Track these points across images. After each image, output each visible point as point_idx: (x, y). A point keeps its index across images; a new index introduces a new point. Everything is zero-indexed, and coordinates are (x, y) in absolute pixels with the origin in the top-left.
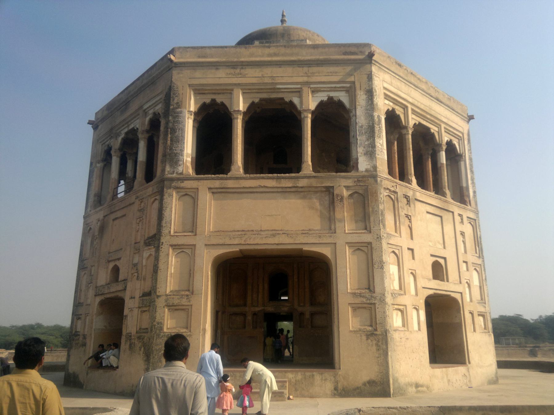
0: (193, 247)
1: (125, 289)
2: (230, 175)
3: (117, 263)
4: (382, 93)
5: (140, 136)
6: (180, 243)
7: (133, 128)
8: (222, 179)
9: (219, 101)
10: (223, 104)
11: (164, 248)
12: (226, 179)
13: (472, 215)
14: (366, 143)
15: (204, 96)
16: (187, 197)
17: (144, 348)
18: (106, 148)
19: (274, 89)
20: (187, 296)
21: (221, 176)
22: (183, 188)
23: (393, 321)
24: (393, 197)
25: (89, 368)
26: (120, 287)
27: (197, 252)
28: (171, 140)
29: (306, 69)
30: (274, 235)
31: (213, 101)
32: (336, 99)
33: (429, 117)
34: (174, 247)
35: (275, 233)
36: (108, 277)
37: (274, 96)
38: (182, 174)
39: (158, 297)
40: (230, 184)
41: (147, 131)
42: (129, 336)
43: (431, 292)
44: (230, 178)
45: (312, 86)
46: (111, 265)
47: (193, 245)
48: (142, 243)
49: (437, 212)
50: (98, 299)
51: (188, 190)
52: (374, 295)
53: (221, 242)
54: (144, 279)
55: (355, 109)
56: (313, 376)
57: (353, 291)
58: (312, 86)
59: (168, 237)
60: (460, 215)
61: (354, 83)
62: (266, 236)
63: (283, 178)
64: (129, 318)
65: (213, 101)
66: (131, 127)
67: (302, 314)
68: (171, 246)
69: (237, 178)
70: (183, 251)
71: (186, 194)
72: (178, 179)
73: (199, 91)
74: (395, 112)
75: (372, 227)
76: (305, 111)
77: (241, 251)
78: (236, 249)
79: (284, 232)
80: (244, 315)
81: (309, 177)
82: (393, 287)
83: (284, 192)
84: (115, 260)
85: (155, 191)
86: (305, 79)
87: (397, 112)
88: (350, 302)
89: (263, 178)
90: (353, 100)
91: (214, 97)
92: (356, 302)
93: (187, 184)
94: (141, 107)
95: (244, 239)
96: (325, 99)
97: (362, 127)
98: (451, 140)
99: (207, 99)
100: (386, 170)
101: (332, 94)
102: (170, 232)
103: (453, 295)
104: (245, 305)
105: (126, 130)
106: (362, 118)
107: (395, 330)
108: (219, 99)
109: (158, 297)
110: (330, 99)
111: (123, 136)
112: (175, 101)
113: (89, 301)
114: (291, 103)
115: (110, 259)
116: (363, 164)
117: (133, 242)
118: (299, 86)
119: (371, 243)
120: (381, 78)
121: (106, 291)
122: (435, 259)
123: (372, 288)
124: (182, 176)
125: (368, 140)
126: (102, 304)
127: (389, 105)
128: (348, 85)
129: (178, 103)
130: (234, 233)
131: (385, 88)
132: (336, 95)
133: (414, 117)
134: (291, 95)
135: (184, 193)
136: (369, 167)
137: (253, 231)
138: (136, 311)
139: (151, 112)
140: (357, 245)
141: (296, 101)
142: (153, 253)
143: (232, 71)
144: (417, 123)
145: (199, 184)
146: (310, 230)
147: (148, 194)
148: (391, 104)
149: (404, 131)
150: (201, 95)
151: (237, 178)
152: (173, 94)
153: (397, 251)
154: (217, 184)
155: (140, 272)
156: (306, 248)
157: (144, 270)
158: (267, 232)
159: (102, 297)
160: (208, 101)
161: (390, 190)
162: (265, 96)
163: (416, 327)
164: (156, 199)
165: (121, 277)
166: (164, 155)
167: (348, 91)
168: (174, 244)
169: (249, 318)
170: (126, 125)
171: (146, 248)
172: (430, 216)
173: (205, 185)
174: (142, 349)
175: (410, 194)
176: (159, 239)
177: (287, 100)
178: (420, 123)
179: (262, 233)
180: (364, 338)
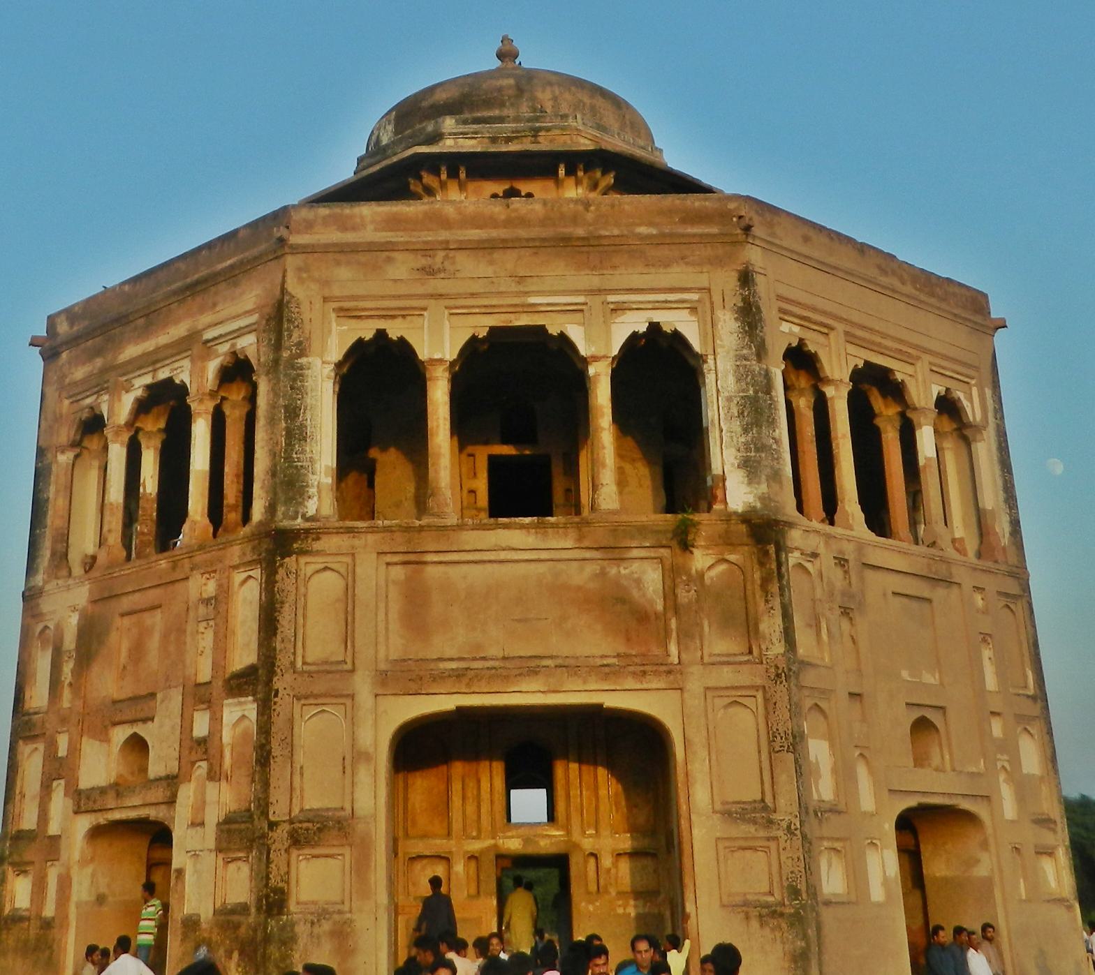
0: (348, 702)
3: (140, 729)
5: (193, 406)
7: (170, 381)
9: (393, 335)
10: (402, 341)
14: (743, 439)
16: (328, 574)
18: (85, 415)
23: (820, 880)
31: (381, 334)
34: (303, 702)
37: (523, 320)
38: (312, 519)
41: (213, 394)
47: (347, 696)
51: (329, 559)
52: (773, 816)
57: (727, 807)
59: (289, 677)
62: (518, 672)
65: (381, 334)
66: (163, 375)
70: (324, 711)
71: (326, 569)
73: (345, 313)
74: (805, 345)
75: (763, 647)
79: (559, 661)
82: (819, 795)
84: (133, 722)
87: (812, 348)
88: (718, 835)
89: (506, 526)
91: (381, 324)
99: (367, 331)
100: (792, 502)
102: (293, 664)
105: (148, 380)
108: (395, 330)
111: (139, 393)
116: (739, 495)
119: (764, 687)
124: (315, 525)
127: (791, 333)
132: (673, 320)
133: (851, 349)
135: (322, 566)
136: (750, 499)
140: (734, 693)
143: (423, 262)
144: (861, 365)
145: (357, 542)
149: (829, 391)
150: (353, 321)
160: (368, 335)
164: (250, 577)
170: (150, 369)
171: (230, 701)
178: (867, 363)
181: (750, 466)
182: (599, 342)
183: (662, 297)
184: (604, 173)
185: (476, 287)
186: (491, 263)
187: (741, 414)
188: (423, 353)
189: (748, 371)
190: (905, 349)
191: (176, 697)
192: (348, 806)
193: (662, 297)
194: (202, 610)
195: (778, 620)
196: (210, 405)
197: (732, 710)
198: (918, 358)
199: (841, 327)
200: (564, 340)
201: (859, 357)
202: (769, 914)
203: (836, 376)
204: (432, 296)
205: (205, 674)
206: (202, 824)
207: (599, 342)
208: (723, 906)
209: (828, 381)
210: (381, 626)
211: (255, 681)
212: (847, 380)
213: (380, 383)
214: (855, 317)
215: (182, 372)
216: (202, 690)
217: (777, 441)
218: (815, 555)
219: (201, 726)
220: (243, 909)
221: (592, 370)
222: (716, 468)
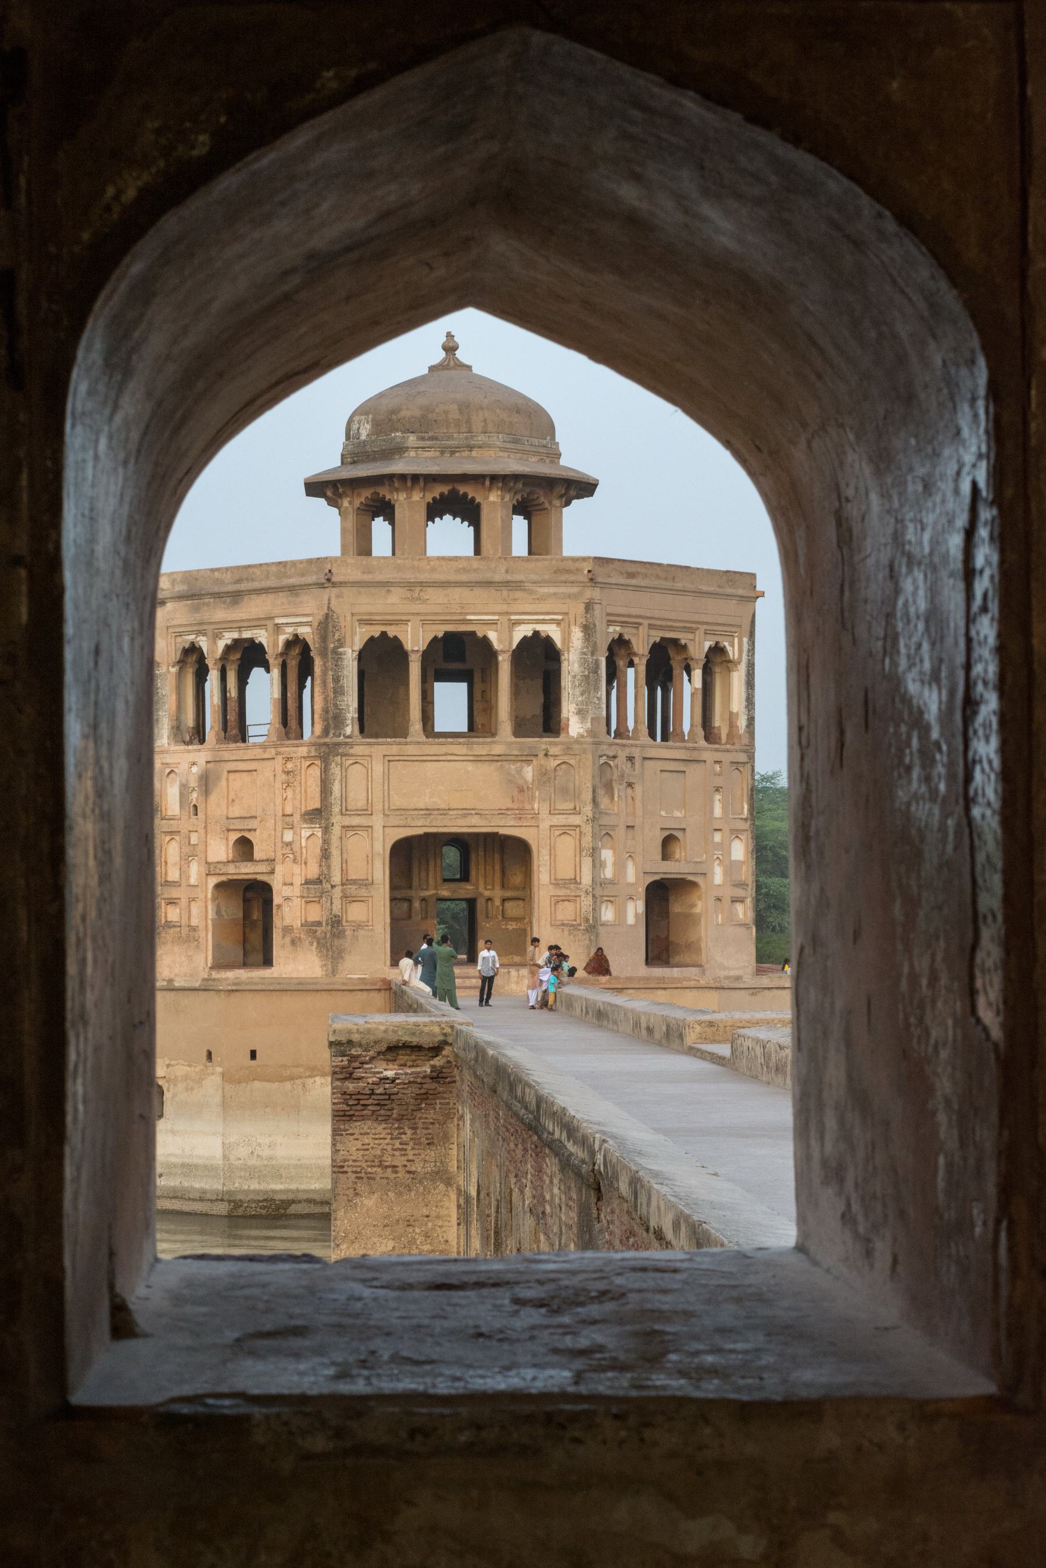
1: (272, 872)
2: (409, 739)
4: (605, 622)
6: (354, 824)
8: (399, 744)
9: (391, 635)
10: (395, 637)
11: (336, 831)
12: (406, 744)
13: (742, 757)
15: (372, 628)
16: (357, 765)
17: (318, 943)
19: (464, 620)
20: (366, 885)
21: (398, 740)
22: (352, 755)
24: (611, 763)
25: (211, 968)
26: (262, 868)
27: (375, 835)
28: (335, 692)
29: (505, 593)
30: (465, 816)
31: (384, 634)
32: (543, 635)
33: (678, 625)
35: (466, 813)
36: (230, 851)
38: (349, 737)
39: (333, 887)
40: (411, 749)
41: (282, 654)
42: (287, 930)
43: (657, 877)
44: (411, 743)
45: (513, 617)
46: (234, 837)
48: (297, 817)
49: (681, 767)
50: (213, 881)
53: (402, 823)
54: (306, 863)
55: (568, 651)
56: (509, 972)
58: (513, 617)
59: (339, 817)
60: (716, 762)
61: (567, 614)
63: (478, 744)
64: (286, 909)
65: (384, 634)
66: (247, 635)
67: (489, 899)
68: (343, 827)
69: (419, 743)
72: (346, 744)
76: (503, 652)
77: (427, 835)
78: (420, 831)
80: (409, 901)
81: (506, 743)
83: (478, 760)
85: (313, 754)
86: (504, 608)
87: (626, 637)
90: (567, 637)
91: (383, 628)
92: (560, 893)
93: (358, 750)
94: (272, 618)
95: (429, 820)
96: (530, 634)
97: (574, 677)
98: (717, 643)
99: (376, 631)
101: (539, 627)
103: (690, 878)
104: (410, 887)
105: (236, 635)
106: (576, 665)
107: (603, 925)
108: (392, 631)
109: (333, 887)
110: (536, 633)
111: (229, 642)
112: (336, 637)
113: (193, 881)
114: (485, 640)
115: (232, 827)
116: (575, 727)
117: (280, 813)
118: (496, 617)
120: (604, 603)
121: (233, 871)
122: (667, 833)
123: (578, 878)
125: (582, 695)
126: (218, 886)
128: (560, 617)
129: (339, 640)
130: (416, 812)
131: (608, 614)
133: (653, 632)
134: (485, 627)
136: (581, 731)
137: (438, 809)
138: (297, 902)
139: (290, 630)
141: (493, 636)
142: (320, 834)
143: (409, 594)
146: (507, 809)
147: (300, 755)
148: (618, 629)
151: (419, 743)
152: (334, 627)
153: (611, 833)
154: (394, 749)
155: (298, 854)
156: (502, 831)
157: (304, 851)
158: (455, 812)
159: (224, 878)
160: (377, 635)
161: (608, 757)
162: (451, 628)
163: (631, 920)
165: (257, 854)
166: (326, 711)
167: (558, 623)
168: (346, 824)
169: (417, 904)
172: (667, 774)
173: (380, 749)
174: (315, 944)
175: (636, 753)
176: (328, 819)
177: (480, 634)
178: (662, 639)
179: (451, 813)
180: (566, 933)
181: (580, 712)
182: (504, 640)
183: (541, 617)
184: (515, 483)
185: (439, 609)
186: (447, 595)
187: (580, 685)
188: (408, 646)
189: (585, 660)
190: (688, 625)
191: (271, 823)
192: (370, 879)
193: (541, 617)
194: (284, 777)
195: (591, 794)
196: (281, 660)
197: (563, 836)
198: (697, 629)
199: (646, 622)
200: (485, 638)
201: (656, 636)
202: (573, 927)
203: (640, 652)
204: (413, 614)
205: (289, 810)
206: (292, 884)
207: (504, 640)
208: (552, 925)
209: (636, 654)
210: (386, 793)
211: (318, 815)
212: (646, 652)
213: (382, 657)
214: (657, 614)
215: (262, 637)
216: (287, 819)
217: (599, 699)
218: (615, 757)
219: (288, 836)
220: (319, 924)
221: (500, 658)
222: (564, 714)
